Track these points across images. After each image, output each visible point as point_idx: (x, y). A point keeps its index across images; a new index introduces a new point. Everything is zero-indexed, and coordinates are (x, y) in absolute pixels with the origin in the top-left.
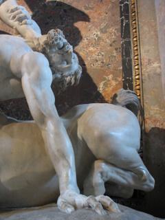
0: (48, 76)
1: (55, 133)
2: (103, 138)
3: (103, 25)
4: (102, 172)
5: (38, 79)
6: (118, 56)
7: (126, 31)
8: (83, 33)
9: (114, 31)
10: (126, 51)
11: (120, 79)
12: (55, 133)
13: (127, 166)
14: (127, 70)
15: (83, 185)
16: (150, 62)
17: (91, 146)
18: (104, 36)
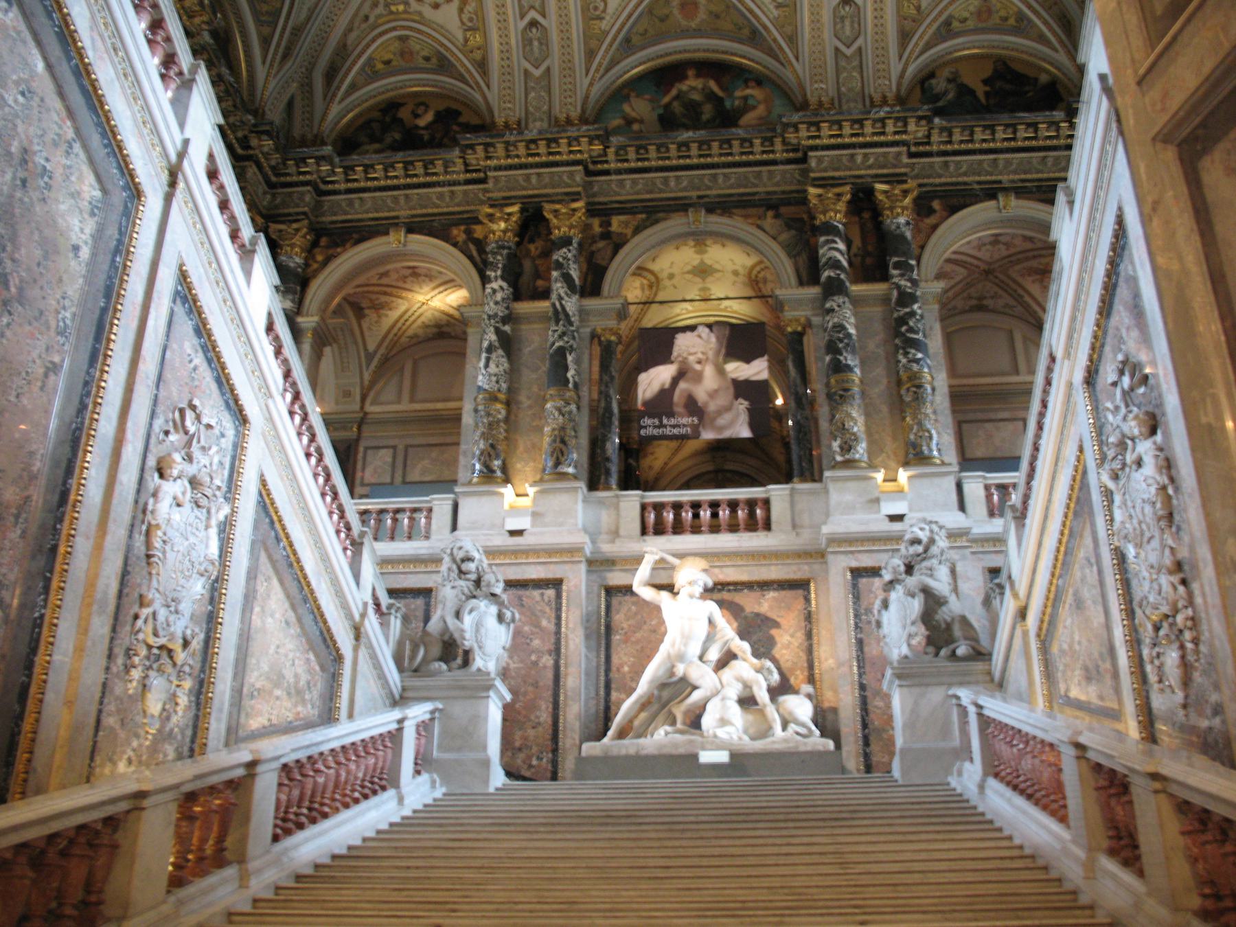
0: (764, 685)
1: (771, 711)
2: (790, 713)
3: (791, 631)
4: (792, 727)
5: (760, 688)
6: (804, 656)
7: (809, 635)
8: (777, 639)
9: (800, 635)
10: (810, 651)
11: (806, 673)
12: (771, 711)
13: (803, 725)
14: (811, 666)
15: (784, 728)
16: (826, 660)
17: (787, 716)
18: (793, 640)
